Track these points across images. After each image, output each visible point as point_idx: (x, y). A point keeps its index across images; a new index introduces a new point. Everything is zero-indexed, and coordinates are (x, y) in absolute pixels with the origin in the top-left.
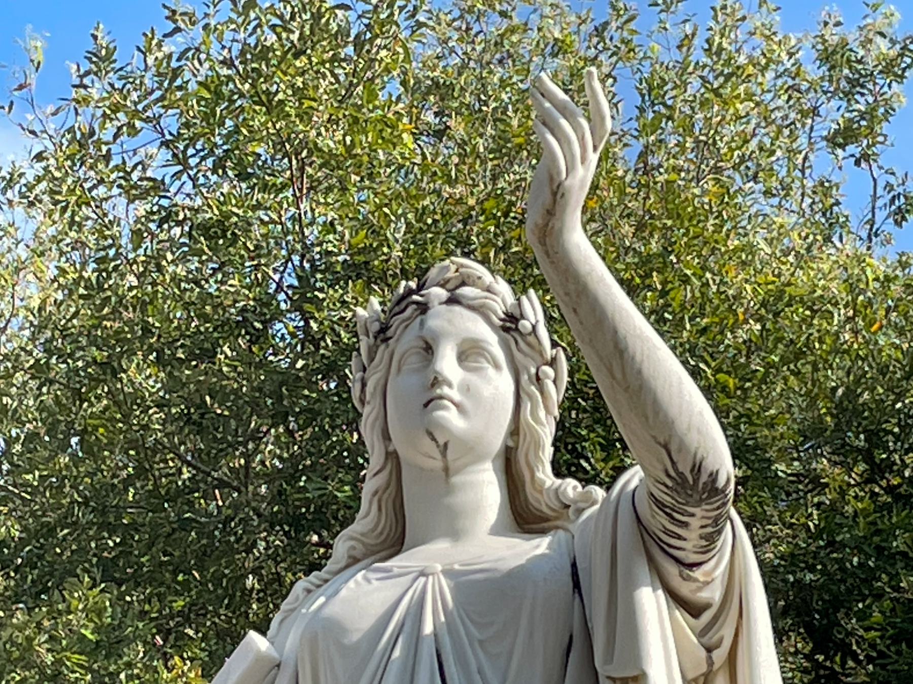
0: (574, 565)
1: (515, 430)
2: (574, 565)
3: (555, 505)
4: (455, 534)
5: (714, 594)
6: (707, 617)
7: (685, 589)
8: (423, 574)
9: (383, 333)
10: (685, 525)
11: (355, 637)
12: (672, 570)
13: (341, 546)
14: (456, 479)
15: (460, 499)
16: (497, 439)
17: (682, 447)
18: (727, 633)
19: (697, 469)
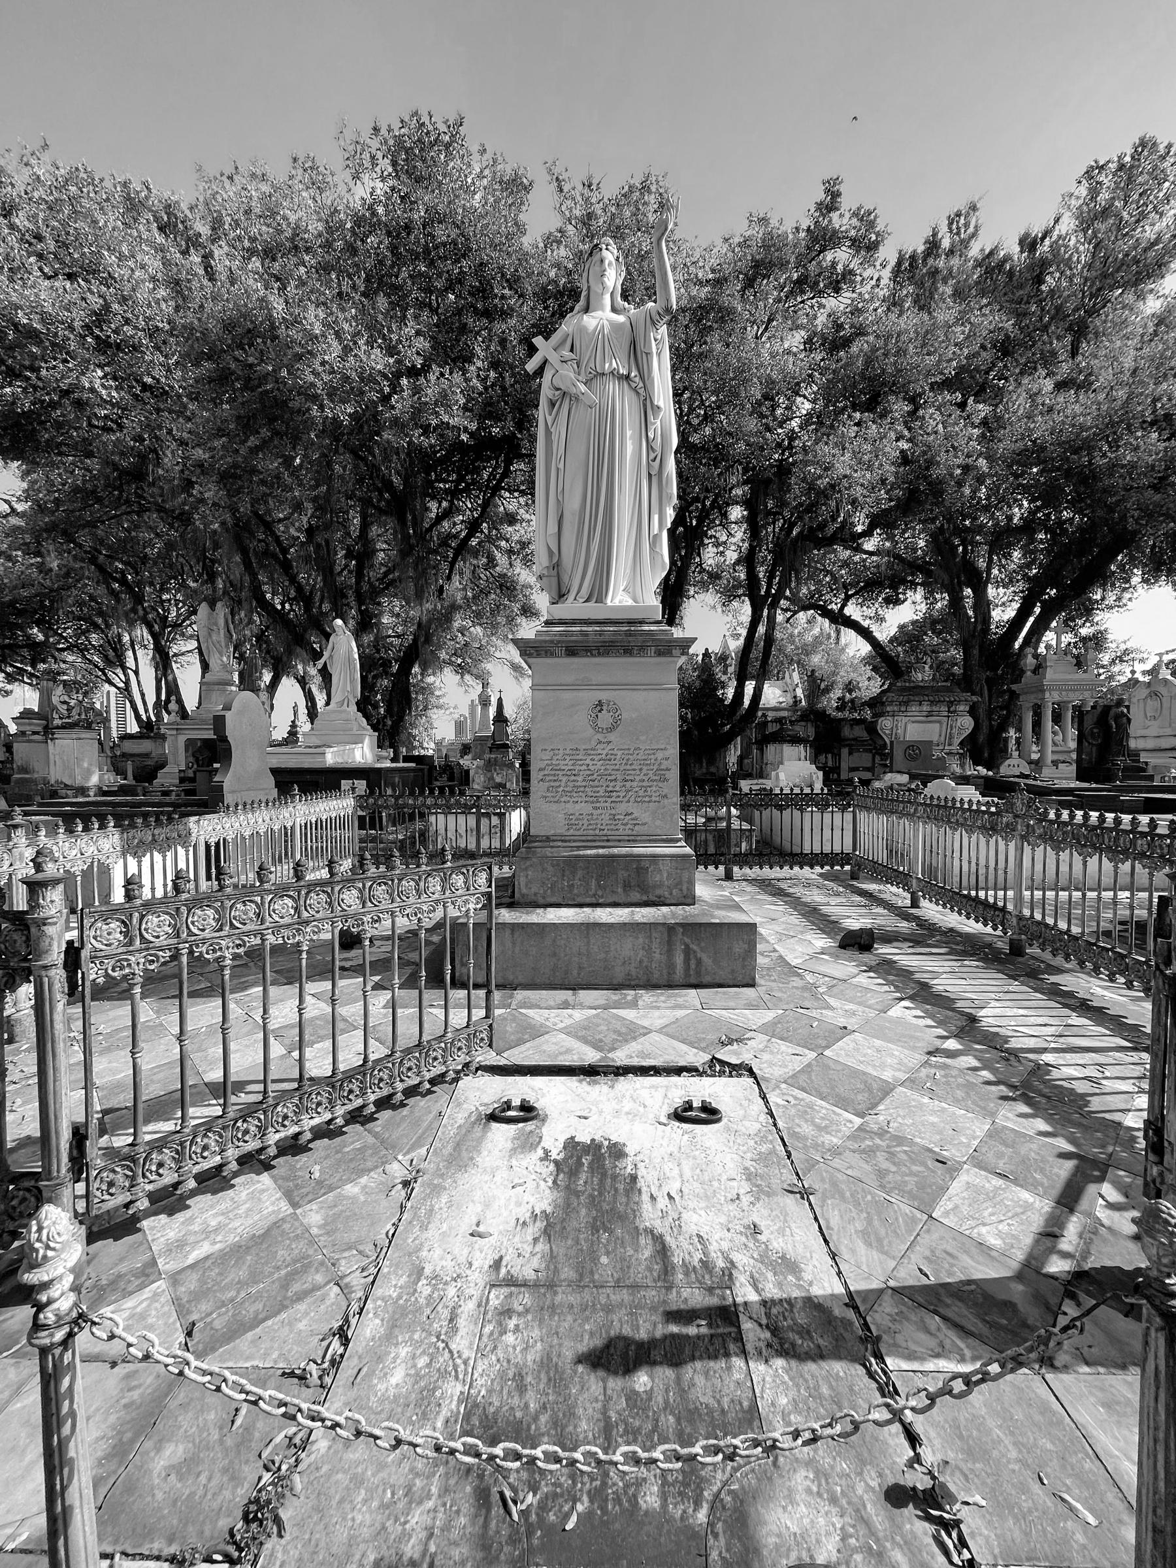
9: (591, 254)
13: (577, 308)
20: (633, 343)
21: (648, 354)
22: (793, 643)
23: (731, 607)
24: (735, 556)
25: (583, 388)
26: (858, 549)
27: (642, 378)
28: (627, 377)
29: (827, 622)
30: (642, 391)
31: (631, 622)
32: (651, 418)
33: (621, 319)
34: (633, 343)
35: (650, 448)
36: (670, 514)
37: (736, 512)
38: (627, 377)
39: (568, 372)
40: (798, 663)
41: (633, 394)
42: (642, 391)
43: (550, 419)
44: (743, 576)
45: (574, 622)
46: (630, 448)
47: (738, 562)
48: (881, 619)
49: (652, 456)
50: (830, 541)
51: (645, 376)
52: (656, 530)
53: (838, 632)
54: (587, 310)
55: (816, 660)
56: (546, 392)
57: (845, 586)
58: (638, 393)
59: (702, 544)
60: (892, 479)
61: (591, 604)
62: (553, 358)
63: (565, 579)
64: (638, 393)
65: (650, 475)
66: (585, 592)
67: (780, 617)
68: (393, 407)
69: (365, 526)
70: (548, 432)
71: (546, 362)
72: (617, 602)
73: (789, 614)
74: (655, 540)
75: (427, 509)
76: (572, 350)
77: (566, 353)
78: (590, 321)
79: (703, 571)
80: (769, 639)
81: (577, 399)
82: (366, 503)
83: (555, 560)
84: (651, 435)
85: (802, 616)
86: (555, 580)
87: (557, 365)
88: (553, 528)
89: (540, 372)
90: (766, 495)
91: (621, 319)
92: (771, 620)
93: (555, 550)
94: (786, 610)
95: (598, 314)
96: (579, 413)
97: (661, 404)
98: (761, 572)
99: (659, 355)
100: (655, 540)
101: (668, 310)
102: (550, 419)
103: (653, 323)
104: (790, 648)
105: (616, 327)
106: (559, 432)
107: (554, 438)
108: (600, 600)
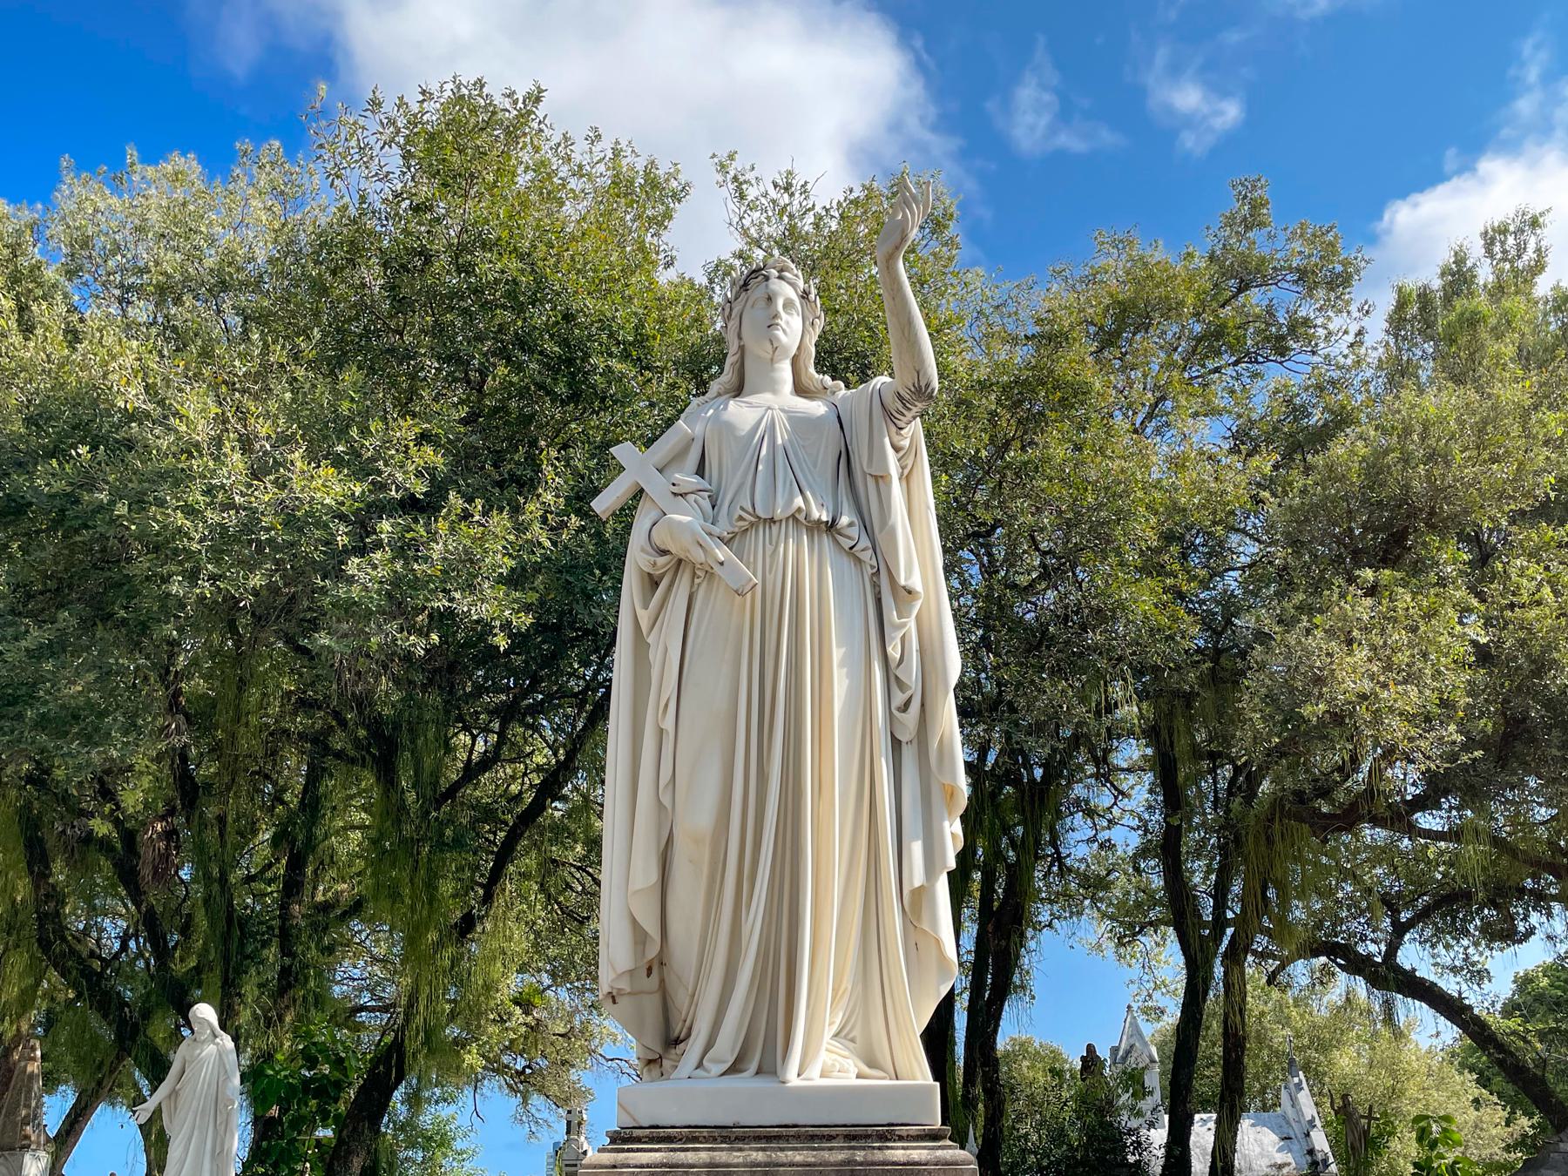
0: (839, 417)
1: (799, 348)
2: (839, 417)
3: (820, 387)
4: (774, 391)
5: (906, 443)
6: (902, 453)
7: (896, 438)
8: (769, 408)
10: (910, 409)
11: (743, 433)
12: (894, 429)
14: (777, 365)
15: (777, 375)
16: (794, 351)
17: (925, 373)
18: (910, 462)
19: (928, 386)
20: (845, 457)
21: (881, 479)
22: (1286, 1022)
23: (1139, 948)
24: (1135, 840)
25: (722, 553)
26: (1413, 831)
27: (866, 527)
28: (831, 526)
29: (1360, 986)
30: (867, 556)
31: (856, 1135)
32: (891, 615)
33: (817, 408)
34: (845, 457)
35: (892, 680)
36: (952, 833)
37: (1130, 752)
38: (831, 526)
39: (684, 517)
40: (1306, 1068)
41: (846, 562)
42: (867, 556)
43: (644, 617)
44: (1157, 882)
45: (692, 1135)
46: (840, 685)
47: (1143, 852)
48: (1479, 975)
49: (899, 698)
50: (1349, 818)
51: (873, 526)
52: (917, 876)
53: (1388, 1007)
54: (738, 390)
55: (1346, 1061)
56: (637, 558)
57: (1390, 904)
58: (858, 561)
59: (1059, 815)
60: (1465, 700)
61: (744, 1082)
62: (656, 487)
63: (681, 999)
64: (858, 561)
65: (896, 744)
66: (726, 1047)
67: (1251, 968)
68: (351, 580)
69: (313, 779)
70: (640, 644)
71: (639, 494)
72: (814, 1079)
73: (1272, 965)
74: (914, 907)
75: (449, 749)
76: (700, 471)
77: (686, 478)
78: (742, 413)
79: (1064, 870)
80: (1235, 1042)
81: (710, 574)
82: (318, 743)
83: (652, 951)
84: (894, 652)
85: (1301, 971)
86: (652, 1004)
87: (664, 501)
88: (645, 874)
89: (625, 515)
90: (1191, 719)
91: (817, 408)
92: (1234, 989)
93: (652, 927)
94: (1263, 956)
95: (765, 398)
96: (712, 605)
97: (916, 583)
98: (1199, 875)
99: (906, 478)
100: (914, 907)
101: (921, 392)
102: (644, 617)
103: (889, 415)
104: (1280, 1036)
105: (800, 423)
106: (666, 643)
107: (655, 656)
108: (770, 1068)
